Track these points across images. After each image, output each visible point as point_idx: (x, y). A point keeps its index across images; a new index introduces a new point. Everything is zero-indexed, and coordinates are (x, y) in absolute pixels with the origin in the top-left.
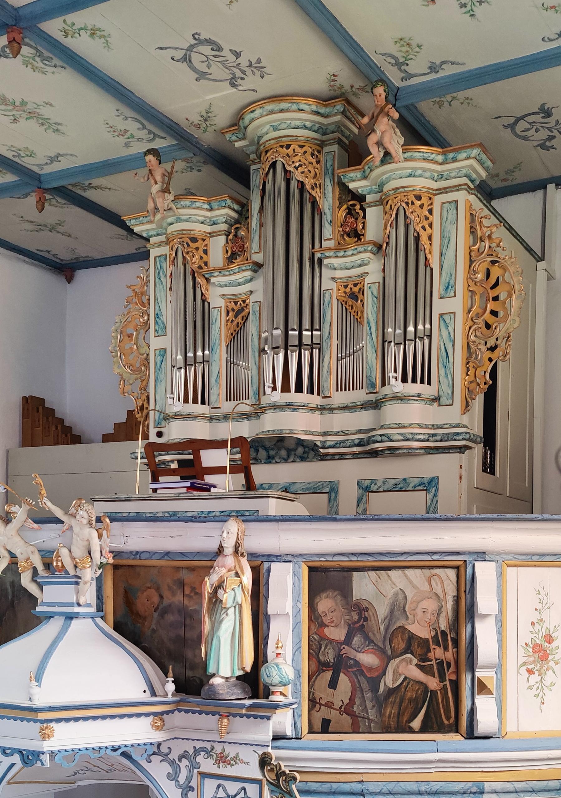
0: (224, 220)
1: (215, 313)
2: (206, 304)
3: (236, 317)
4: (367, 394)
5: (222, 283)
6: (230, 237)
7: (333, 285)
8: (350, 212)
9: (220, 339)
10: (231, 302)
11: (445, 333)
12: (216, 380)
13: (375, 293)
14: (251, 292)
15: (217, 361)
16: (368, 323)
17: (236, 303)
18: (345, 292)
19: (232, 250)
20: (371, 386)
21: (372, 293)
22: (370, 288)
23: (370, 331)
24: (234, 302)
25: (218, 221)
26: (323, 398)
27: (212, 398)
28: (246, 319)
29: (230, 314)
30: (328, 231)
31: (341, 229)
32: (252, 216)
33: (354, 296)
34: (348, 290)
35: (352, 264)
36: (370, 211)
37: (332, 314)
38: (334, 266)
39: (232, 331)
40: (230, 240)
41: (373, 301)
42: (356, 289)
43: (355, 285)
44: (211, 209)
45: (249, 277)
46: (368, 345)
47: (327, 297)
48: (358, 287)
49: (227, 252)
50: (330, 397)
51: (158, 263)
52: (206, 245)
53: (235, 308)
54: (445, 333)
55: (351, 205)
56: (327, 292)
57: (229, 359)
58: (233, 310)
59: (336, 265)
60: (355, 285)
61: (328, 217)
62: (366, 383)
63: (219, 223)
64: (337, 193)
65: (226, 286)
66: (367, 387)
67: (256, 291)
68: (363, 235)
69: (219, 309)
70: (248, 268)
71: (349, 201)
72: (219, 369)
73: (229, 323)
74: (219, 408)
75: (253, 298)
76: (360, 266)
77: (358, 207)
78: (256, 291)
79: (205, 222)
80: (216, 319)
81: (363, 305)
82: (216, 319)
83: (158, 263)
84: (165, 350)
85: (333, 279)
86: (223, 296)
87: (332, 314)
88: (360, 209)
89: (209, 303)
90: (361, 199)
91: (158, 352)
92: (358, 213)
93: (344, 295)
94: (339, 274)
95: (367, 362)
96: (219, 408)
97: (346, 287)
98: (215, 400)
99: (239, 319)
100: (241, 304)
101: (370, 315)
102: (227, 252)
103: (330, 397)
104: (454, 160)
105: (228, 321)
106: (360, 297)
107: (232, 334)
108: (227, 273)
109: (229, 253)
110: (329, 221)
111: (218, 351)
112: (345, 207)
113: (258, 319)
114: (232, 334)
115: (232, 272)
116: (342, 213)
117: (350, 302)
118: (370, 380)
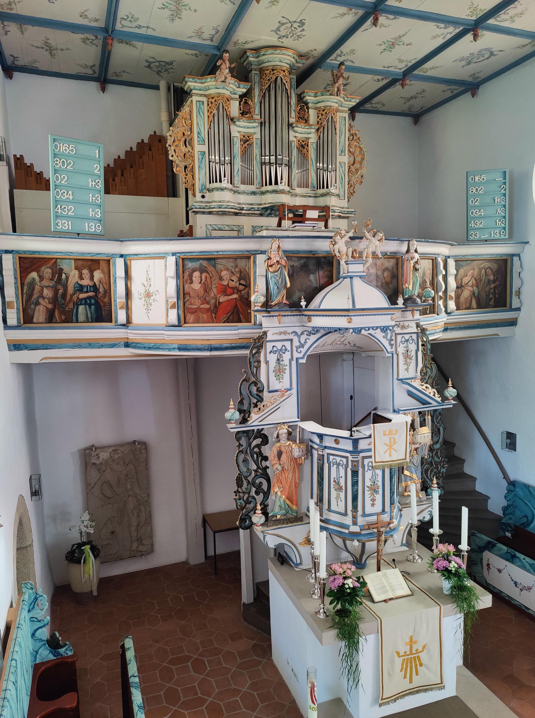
1: (235, 139)
6: (242, 103)
7: (295, 139)
11: (341, 170)
17: (244, 137)
28: (251, 145)
30: (293, 114)
32: (255, 96)
36: (310, 110)
37: (295, 152)
42: (303, 143)
43: (303, 141)
44: (239, 87)
47: (293, 145)
49: (240, 110)
51: (198, 105)
53: (244, 139)
54: (341, 170)
60: (303, 141)
61: (293, 107)
81: (308, 151)
83: (198, 105)
84: (204, 152)
90: (306, 104)
91: (200, 153)
94: (297, 135)
97: (299, 141)
99: (246, 145)
102: (240, 110)
104: (350, 101)
106: (306, 147)
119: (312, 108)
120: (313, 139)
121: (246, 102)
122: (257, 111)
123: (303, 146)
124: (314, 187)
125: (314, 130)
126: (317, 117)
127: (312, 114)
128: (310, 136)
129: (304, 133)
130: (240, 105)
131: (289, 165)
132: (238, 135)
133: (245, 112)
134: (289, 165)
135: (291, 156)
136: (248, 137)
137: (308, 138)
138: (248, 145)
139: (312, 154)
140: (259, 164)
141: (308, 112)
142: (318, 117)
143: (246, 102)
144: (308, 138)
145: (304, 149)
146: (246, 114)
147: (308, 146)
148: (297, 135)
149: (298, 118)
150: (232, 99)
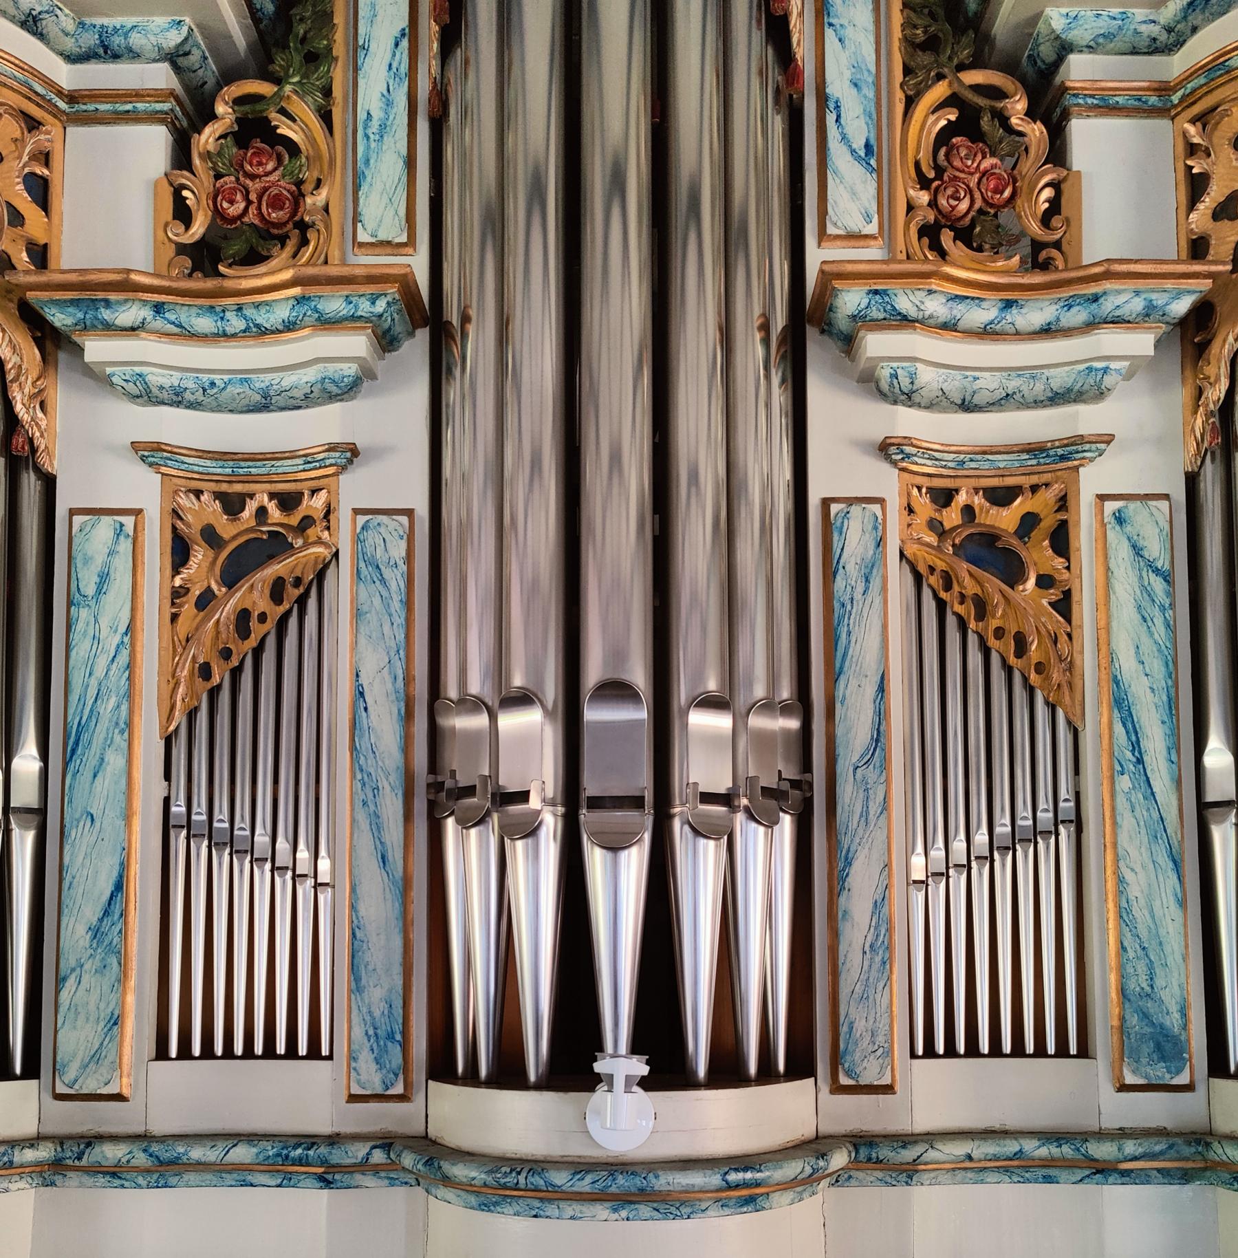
0: (173, 38)
2: (30, 486)
3: (231, 578)
4: (1124, 1088)
5: (156, 378)
6: (207, 138)
7: (885, 481)
8: (970, 122)
9: (130, 695)
10: (198, 493)
12: (96, 933)
13: (1155, 549)
14: (353, 452)
15: (110, 820)
16: (1121, 703)
17: (232, 504)
18: (934, 525)
19: (218, 213)
20: (1158, 1047)
21: (1137, 550)
22: (1120, 519)
23: (1136, 746)
24: (218, 496)
25: (136, 40)
26: (837, 1089)
27: (72, 1038)
29: (199, 556)
30: (851, 197)
31: (924, 197)
32: (356, 49)
33: (996, 556)
34: (952, 517)
35: (1013, 384)
36: (1086, 134)
37: (881, 631)
38: (912, 378)
39: (202, 651)
40: (207, 156)
41: (1147, 590)
42: (1006, 519)
43: (1001, 497)
45: (351, 370)
46: (1127, 822)
47: (854, 542)
48: (1020, 506)
49: (183, 214)
50: (888, 1089)
52: (45, 158)
53: (225, 527)
55: (976, 88)
56: (856, 510)
57: (178, 809)
58: (211, 536)
59: (928, 378)
60: (1001, 497)
61: (854, 119)
62: (1122, 1029)
63: (134, 55)
64: (897, 19)
65: (177, 399)
66: (1125, 1050)
67: (378, 453)
68: (1057, 245)
69: (129, 521)
70: (365, 307)
71: (961, 67)
72: (124, 867)
73: (188, 608)
74: (119, 1097)
75: (354, 490)
76: (1057, 398)
77: (1017, 106)
78: (378, 453)
79: (48, 24)
80: (104, 578)
81: (1064, 606)
82: (104, 578)
85: (886, 449)
86: (150, 453)
87: (881, 631)
88: (1031, 114)
89: (49, 483)
92: (1021, 134)
93: (931, 539)
94: (907, 422)
95: (1124, 914)
96: (119, 1097)
97: (944, 497)
98: (82, 1054)
99: (253, 593)
100: (262, 512)
101: (1127, 664)
102: (183, 214)
103: (888, 1089)
105: (178, 594)
106: (1039, 556)
107: (205, 671)
108: (205, 324)
109: (198, 228)
110: (859, 144)
111: (115, 761)
112: (940, 91)
113: (396, 605)
114: (205, 671)
115: (236, 323)
116: (930, 120)
117: (968, 578)
118: (1145, 1016)
119: (1106, 107)
120: (1137, 444)
121: (254, 130)
122: (383, 203)
123: (996, 550)
124: (1167, 1047)
125: (1142, 343)
126: (1172, 193)
127: (1117, 180)
128: (1085, 419)
129: (1005, 401)
130: (182, 157)
131: (801, 794)
132: (143, 489)
133: (236, 236)
134: (801, 794)
135: (833, 676)
136: (288, 502)
137: (1068, 453)
138: (277, 590)
139: (1124, 622)
140: (392, 806)
141: (1057, 153)
142: (1196, 186)
143: (254, 130)
144: (1068, 453)
145: (1012, 571)
146: (253, 258)
147: (1061, 541)
148: (907, 422)
149: (929, 233)
150: (82, 108)
